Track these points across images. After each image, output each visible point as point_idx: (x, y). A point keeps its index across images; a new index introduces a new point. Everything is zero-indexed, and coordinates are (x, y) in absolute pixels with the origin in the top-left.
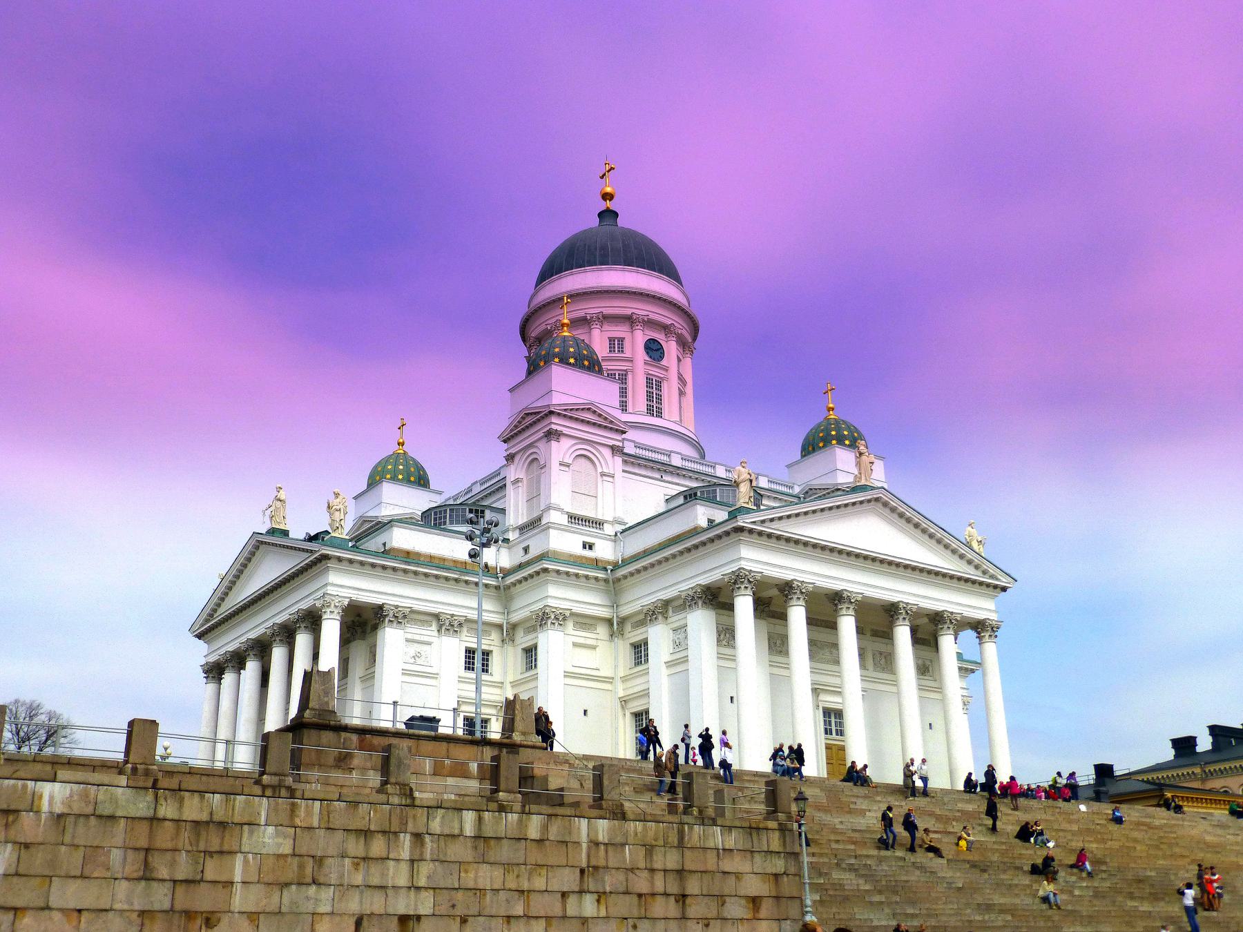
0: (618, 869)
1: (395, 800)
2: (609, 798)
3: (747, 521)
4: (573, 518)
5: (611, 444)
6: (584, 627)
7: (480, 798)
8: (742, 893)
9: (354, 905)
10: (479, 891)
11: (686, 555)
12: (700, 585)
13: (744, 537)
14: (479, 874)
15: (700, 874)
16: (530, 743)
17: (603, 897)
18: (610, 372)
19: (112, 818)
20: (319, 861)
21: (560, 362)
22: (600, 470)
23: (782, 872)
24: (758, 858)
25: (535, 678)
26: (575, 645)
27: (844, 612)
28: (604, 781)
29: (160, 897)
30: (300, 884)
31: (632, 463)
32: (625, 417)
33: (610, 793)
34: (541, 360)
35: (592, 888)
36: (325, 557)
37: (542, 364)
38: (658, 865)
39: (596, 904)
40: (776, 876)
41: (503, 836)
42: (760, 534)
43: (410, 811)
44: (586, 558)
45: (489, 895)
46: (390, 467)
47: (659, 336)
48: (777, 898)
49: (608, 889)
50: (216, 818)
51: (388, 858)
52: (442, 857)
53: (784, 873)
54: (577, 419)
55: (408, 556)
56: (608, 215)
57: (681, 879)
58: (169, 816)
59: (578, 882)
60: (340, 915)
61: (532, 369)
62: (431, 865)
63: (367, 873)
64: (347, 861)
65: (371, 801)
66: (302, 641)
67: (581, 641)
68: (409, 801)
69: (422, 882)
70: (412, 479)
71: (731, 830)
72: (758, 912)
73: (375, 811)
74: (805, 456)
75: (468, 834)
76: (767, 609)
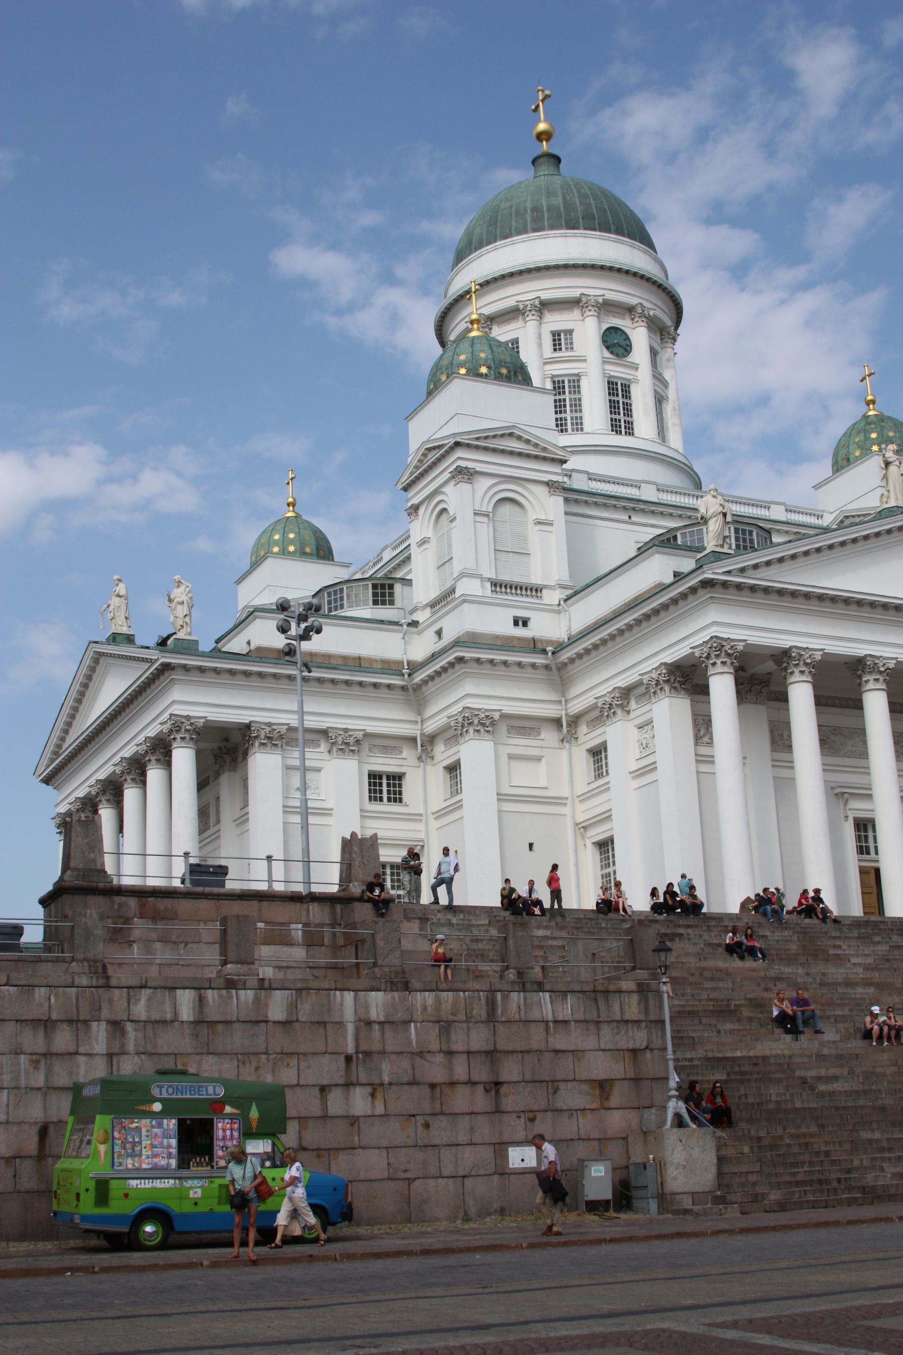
0: (400, 1053)
2: (385, 963)
3: (720, 571)
4: (496, 585)
5: (546, 480)
6: (523, 732)
7: (308, 970)
8: (584, 1076)
9: (35, 1111)
11: (644, 624)
12: (665, 664)
13: (718, 593)
14: (203, 1069)
15: (520, 1056)
17: (380, 1090)
18: (556, 379)
21: (468, 373)
23: (644, 1047)
24: (606, 1030)
25: (458, 806)
26: (511, 757)
27: (871, 685)
28: (378, 941)
31: (586, 502)
32: (565, 440)
33: (386, 956)
34: (442, 373)
35: (363, 1079)
37: (444, 378)
38: (458, 1042)
39: (370, 1098)
40: (634, 1052)
41: (234, 1018)
42: (739, 587)
43: (104, 994)
44: (519, 639)
48: (636, 1080)
49: (386, 1079)
51: (77, 1053)
52: (150, 1049)
53: (647, 1048)
54: (494, 450)
57: (492, 1062)
59: (342, 1073)
60: (19, 1124)
61: (432, 387)
62: (136, 1058)
65: (50, 984)
68: (101, 982)
70: (308, 550)
71: (566, 996)
72: (607, 1099)
73: (56, 995)
74: (837, 471)
76: (765, 690)
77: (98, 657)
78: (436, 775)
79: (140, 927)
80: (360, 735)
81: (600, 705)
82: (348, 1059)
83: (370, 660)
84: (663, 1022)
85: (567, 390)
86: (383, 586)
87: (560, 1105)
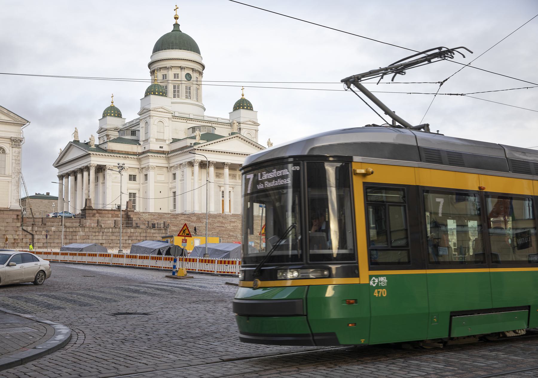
1: (99, 227)
9: (94, 242)
10: (112, 240)
20: (89, 236)
22: (165, 125)
26: (157, 174)
27: (225, 168)
36: (90, 154)
42: (201, 150)
44: (160, 151)
46: (109, 112)
47: (190, 72)
50: (74, 231)
55: (112, 152)
56: (176, 26)
58: (68, 231)
66: (85, 174)
70: (116, 115)
77: (71, 145)
79: (97, 215)
83: (130, 152)
86: (133, 132)
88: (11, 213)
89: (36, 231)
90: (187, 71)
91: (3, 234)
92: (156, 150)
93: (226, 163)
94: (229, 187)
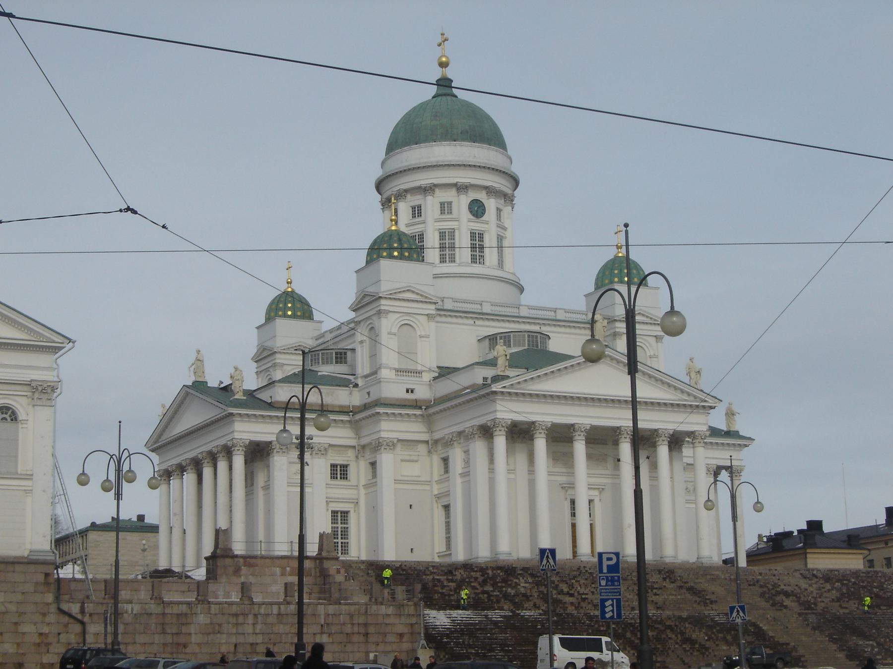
0: (337, 624)
1: (246, 602)
3: (500, 387)
4: (397, 370)
9: (233, 640)
16: (331, 557)
18: (441, 231)
19: (151, 614)
20: (220, 625)
26: (402, 461)
27: (577, 438)
29: (169, 639)
30: (214, 633)
36: (231, 414)
38: (355, 622)
40: (412, 625)
42: (509, 393)
45: (284, 636)
47: (481, 196)
49: (333, 632)
54: (399, 299)
63: (237, 629)
64: (230, 625)
66: (222, 465)
67: (407, 458)
69: (258, 631)
75: (275, 613)
77: (187, 394)
78: (363, 465)
80: (326, 446)
81: (446, 438)
82: (322, 625)
83: (333, 406)
84: (420, 615)
85: (447, 238)
86: (341, 353)
87: (387, 641)
88: (32, 568)
89: (91, 615)
90: (473, 195)
91: (14, 621)
92: (397, 400)
93: (576, 427)
94: (589, 488)
